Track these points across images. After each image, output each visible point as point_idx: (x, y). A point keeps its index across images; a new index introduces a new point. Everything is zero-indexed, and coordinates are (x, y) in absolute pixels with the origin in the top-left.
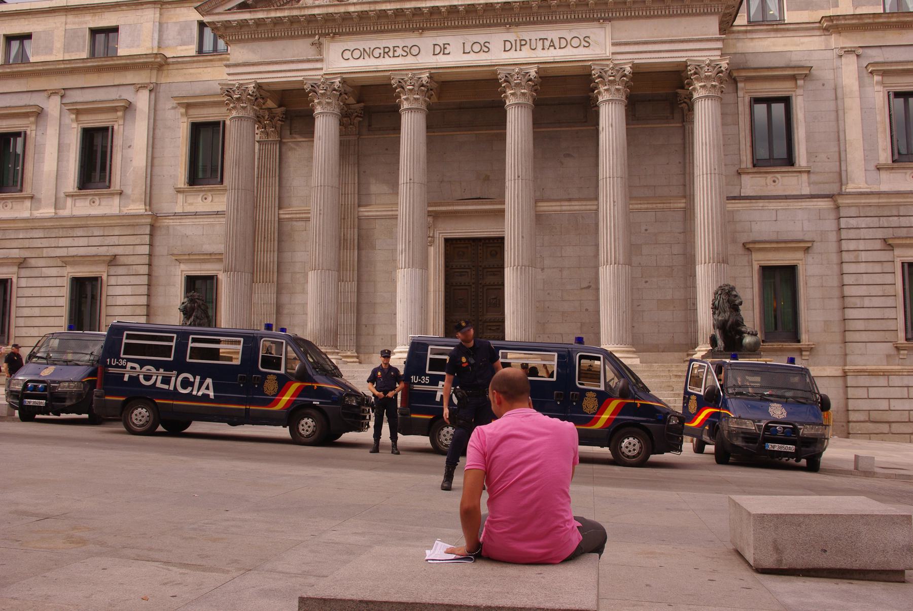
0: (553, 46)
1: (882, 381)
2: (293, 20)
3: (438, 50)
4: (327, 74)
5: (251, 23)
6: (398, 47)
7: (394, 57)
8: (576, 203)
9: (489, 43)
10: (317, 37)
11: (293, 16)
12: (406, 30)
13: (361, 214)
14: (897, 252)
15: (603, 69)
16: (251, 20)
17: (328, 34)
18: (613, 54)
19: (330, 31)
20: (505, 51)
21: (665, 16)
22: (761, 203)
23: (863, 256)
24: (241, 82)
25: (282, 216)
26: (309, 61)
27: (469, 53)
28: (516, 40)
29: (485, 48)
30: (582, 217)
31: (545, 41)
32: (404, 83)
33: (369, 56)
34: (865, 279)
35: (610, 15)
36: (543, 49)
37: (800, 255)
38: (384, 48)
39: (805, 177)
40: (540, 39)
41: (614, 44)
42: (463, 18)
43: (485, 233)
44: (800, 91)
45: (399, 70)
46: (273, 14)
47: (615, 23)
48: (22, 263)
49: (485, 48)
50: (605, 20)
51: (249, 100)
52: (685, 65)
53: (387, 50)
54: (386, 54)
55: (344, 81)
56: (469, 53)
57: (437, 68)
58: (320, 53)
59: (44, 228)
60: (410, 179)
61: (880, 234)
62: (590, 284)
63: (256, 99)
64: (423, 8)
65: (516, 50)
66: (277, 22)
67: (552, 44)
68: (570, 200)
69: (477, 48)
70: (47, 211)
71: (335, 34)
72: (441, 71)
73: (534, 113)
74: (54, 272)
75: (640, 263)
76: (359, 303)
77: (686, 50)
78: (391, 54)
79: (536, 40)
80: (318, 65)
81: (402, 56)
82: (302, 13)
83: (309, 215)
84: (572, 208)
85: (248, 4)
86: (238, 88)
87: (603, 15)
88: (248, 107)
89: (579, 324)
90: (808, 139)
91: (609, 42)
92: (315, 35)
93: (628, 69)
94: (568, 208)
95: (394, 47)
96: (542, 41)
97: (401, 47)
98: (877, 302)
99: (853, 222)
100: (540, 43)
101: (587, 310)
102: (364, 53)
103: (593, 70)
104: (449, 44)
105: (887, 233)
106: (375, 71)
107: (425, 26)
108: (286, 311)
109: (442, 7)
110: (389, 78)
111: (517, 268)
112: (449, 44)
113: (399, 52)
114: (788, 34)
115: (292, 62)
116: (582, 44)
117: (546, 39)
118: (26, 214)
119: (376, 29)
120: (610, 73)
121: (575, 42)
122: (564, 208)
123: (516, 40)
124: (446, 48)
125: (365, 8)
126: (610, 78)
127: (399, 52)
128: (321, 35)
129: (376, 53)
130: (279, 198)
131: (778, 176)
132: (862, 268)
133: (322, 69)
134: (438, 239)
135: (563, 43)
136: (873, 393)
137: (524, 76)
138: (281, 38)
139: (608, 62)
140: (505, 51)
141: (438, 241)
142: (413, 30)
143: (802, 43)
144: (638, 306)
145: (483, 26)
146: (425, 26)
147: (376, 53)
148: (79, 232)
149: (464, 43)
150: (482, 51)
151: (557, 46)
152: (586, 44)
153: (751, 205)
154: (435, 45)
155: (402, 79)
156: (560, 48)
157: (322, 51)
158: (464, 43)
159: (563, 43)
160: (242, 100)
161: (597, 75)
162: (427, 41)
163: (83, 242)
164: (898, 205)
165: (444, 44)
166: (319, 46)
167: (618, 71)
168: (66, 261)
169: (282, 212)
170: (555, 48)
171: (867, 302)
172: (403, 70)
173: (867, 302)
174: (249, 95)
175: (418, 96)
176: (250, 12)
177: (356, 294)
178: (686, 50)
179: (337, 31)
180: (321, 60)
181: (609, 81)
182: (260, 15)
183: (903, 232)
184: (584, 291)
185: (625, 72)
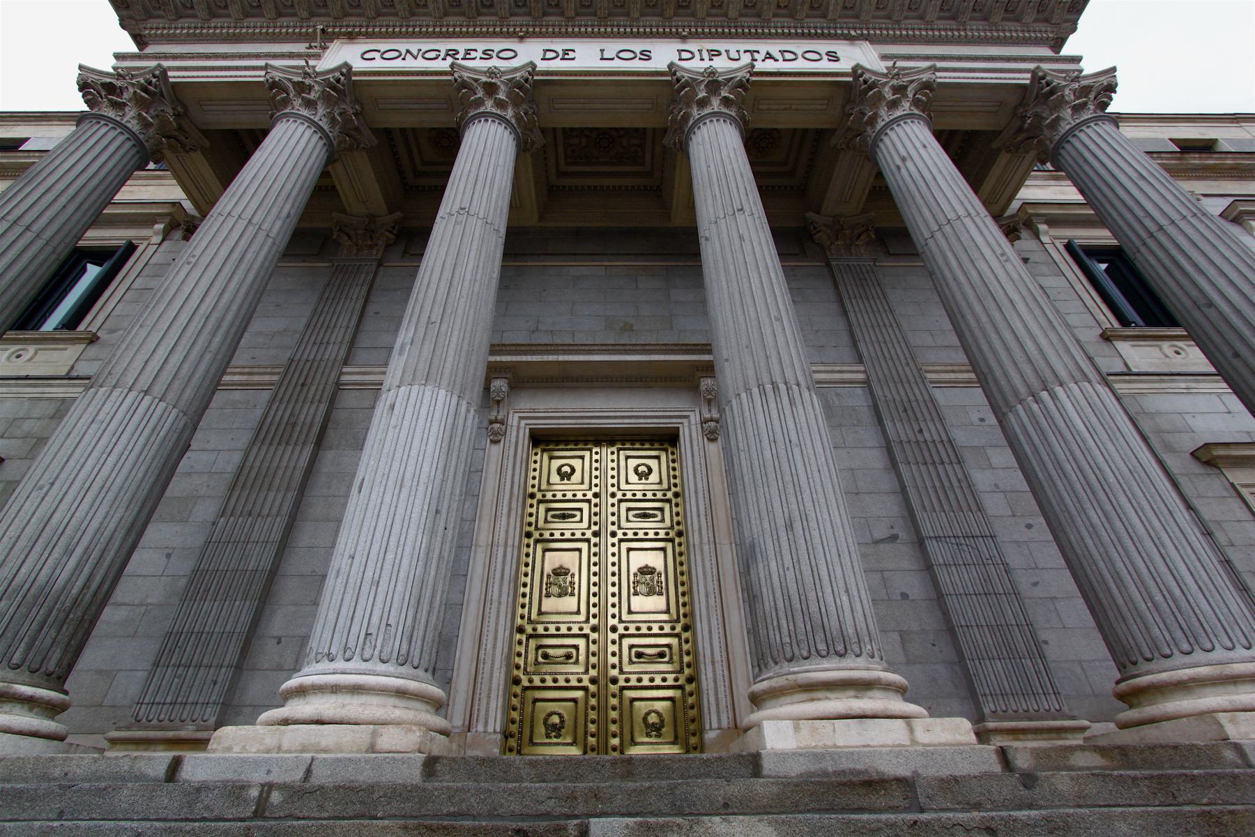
13: (345, 378)
22: (1182, 384)
27: (613, 59)
30: (837, 395)
31: (755, 54)
40: (745, 52)
56: (613, 59)
62: (895, 531)
75: (996, 486)
76: (273, 574)
89: (896, 636)
101: (905, 596)
134: (515, 429)
141: (514, 434)
144: (1036, 584)
153: (1164, 385)
177: (274, 549)
184: (881, 546)
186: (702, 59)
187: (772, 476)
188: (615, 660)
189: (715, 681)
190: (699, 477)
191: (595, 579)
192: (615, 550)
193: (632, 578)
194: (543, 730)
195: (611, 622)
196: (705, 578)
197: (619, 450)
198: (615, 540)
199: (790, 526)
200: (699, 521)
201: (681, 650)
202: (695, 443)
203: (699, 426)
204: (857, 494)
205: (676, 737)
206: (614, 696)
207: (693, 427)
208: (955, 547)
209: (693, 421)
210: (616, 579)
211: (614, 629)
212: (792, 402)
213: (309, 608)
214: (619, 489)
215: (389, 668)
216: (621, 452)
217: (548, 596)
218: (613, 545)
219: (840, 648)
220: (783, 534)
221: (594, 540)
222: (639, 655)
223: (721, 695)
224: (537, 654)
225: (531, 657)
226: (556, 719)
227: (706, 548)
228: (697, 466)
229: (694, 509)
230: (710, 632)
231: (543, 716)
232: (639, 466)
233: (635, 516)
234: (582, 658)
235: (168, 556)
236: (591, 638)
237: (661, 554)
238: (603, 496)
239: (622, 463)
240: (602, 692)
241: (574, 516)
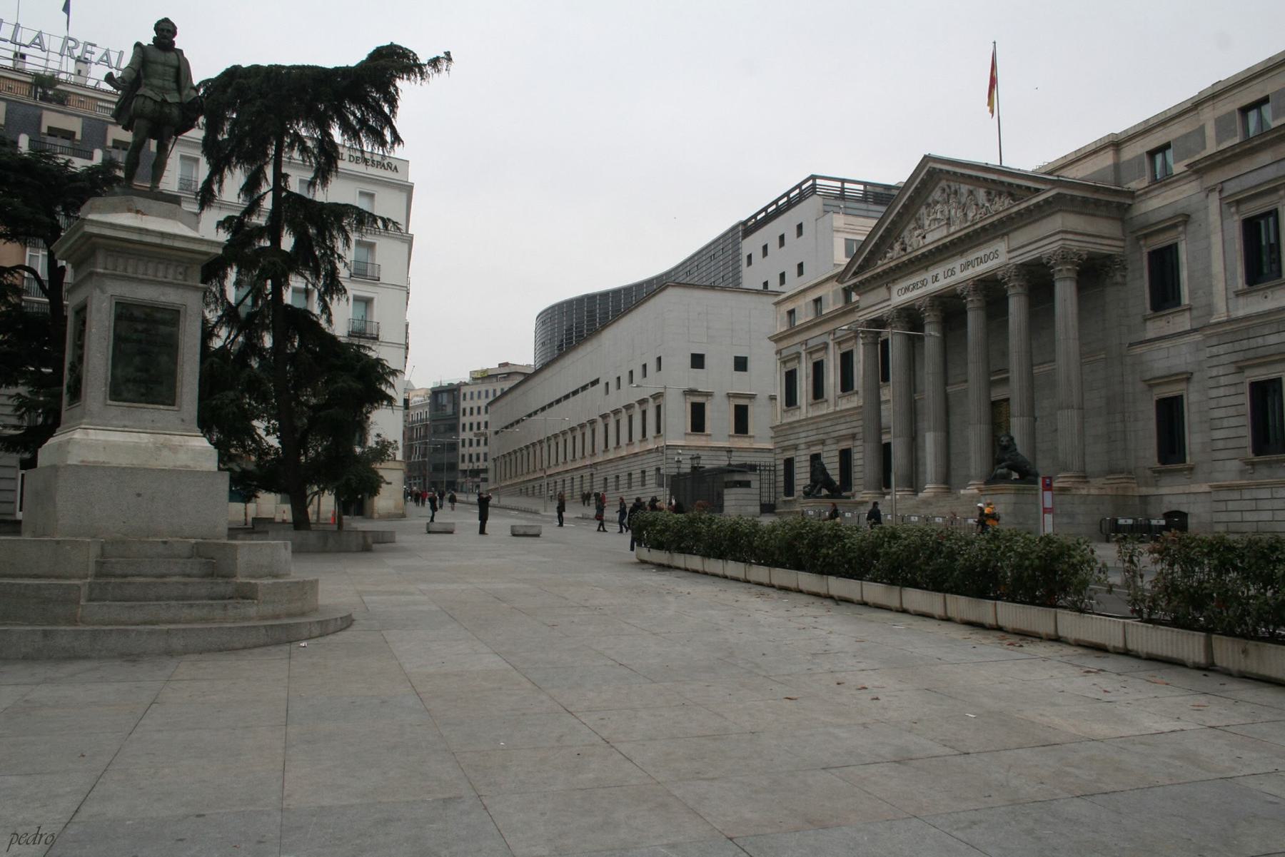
1: (1236, 495)
2: (873, 277)
14: (1248, 373)
18: (1010, 259)
22: (1158, 344)
23: (1223, 381)
26: (885, 301)
29: (953, 272)
34: (1224, 402)
37: (1183, 386)
39: (1187, 314)
44: (1183, 237)
48: (823, 442)
50: (1003, 235)
52: (1040, 258)
59: (831, 419)
61: (1234, 358)
70: (831, 409)
74: (834, 447)
90: (1190, 277)
98: (1233, 422)
99: (1215, 350)
102: (907, 289)
105: (1240, 356)
110: (914, 305)
113: (920, 285)
114: (1173, 186)
118: (825, 412)
127: (920, 285)
131: (1170, 317)
132: (1222, 392)
136: (1231, 506)
142: (922, 268)
143: (1184, 191)
148: (842, 420)
162: (928, 275)
163: (843, 426)
164: (1248, 328)
166: (889, 289)
168: (839, 439)
171: (1226, 423)
173: (1226, 423)
182: (860, 278)
183: (1251, 354)
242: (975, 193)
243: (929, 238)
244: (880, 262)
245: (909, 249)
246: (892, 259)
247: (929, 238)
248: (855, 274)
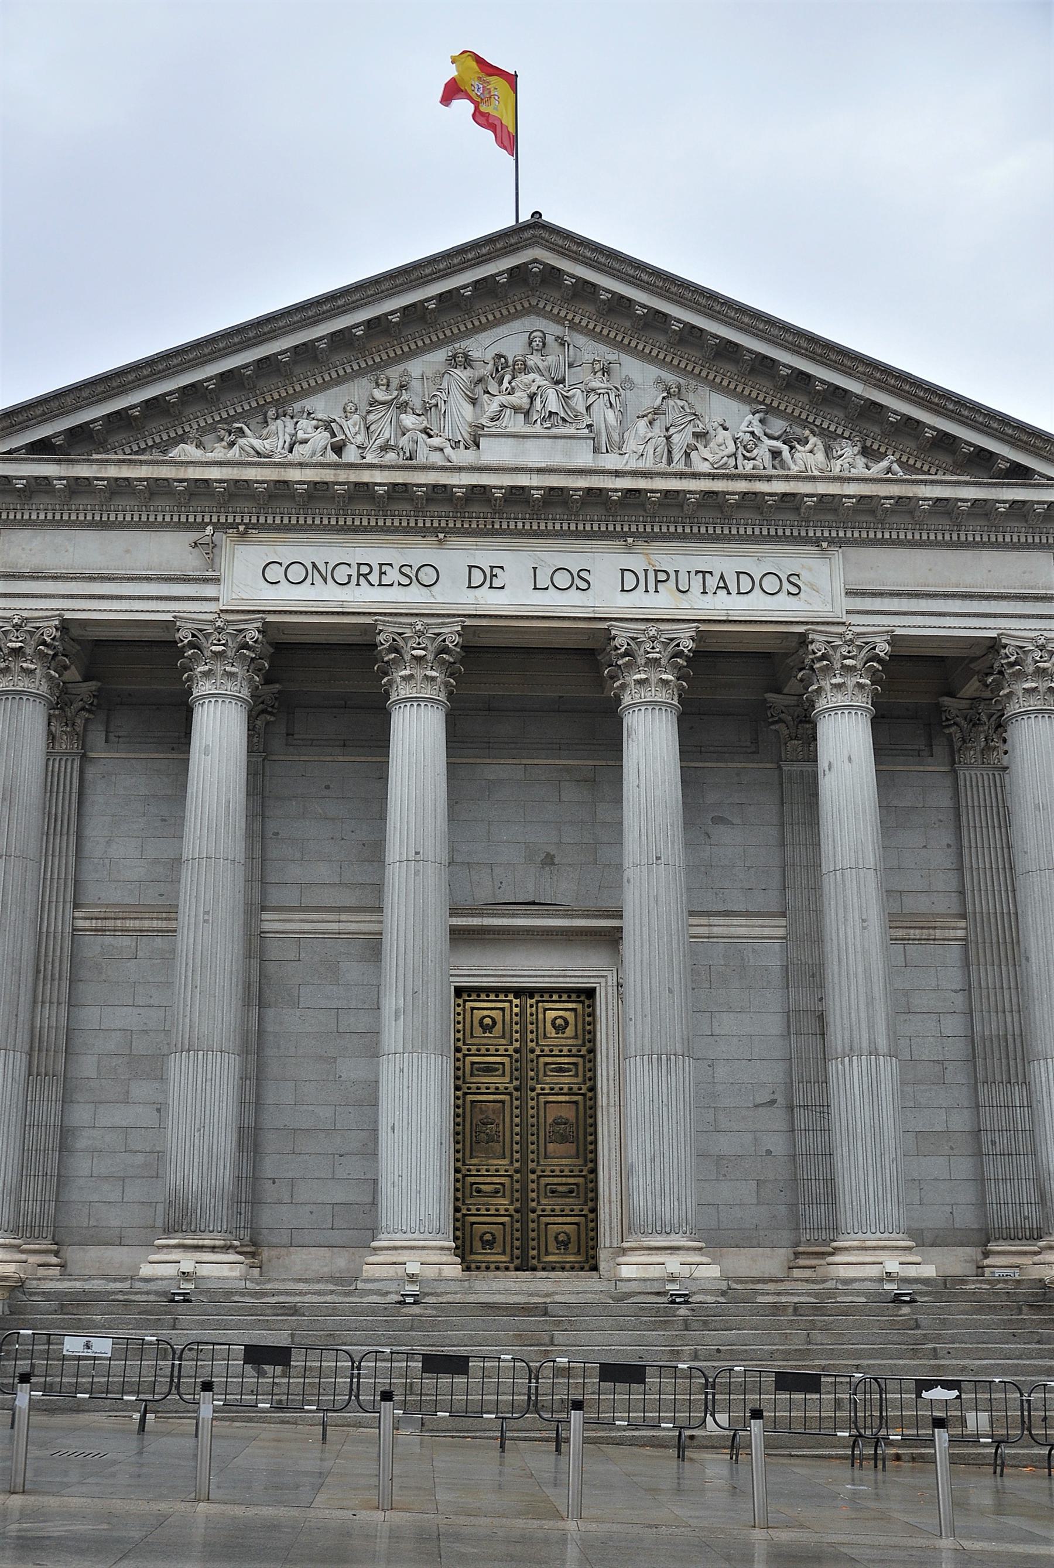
0: (726, 587)
2: (158, 488)
3: (477, 577)
4: (227, 611)
5: (59, 485)
6: (391, 565)
7: (380, 585)
8: (742, 921)
9: (589, 571)
10: (209, 530)
11: (157, 479)
12: (407, 531)
13: (267, 926)
15: (829, 643)
16: (61, 478)
17: (234, 526)
18: (848, 612)
19: (238, 520)
20: (623, 590)
21: (950, 545)
24: (26, 614)
25: (80, 924)
26: (186, 579)
27: (547, 589)
28: (646, 571)
30: (754, 951)
31: (707, 575)
32: (401, 643)
33: (325, 580)
35: (841, 534)
36: (704, 592)
38: (359, 564)
40: (697, 572)
41: (850, 593)
42: (536, 515)
43: (547, 980)
45: (391, 614)
46: (113, 472)
47: (852, 552)
49: (581, 581)
50: (832, 542)
51: (42, 655)
53: (365, 570)
54: (362, 579)
55: (266, 629)
56: (547, 589)
57: (475, 616)
58: (212, 564)
60: (417, 853)
62: (775, 1097)
63: (55, 655)
64: (455, 486)
65: (647, 591)
66: (120, 487)
67: (722, 584)
68: (727, 914)
69: (562, 580)
71: (248, 526)
72: (484, 622)
73: (683, 720)
77: (995, 616)
78: (374, 578)
79: (689, 572)
80: (209, 591)
81: (400, 584)
82: (181, 476)
83: (173, 924)
84: (733, 931)
85: (53, 445)
86: (17, 627)
87: (826, 534)
88: (38, 671)
91: (839, 588)
92: (207, 524)
93: (883, 649)
94: (724, 931)
95: (381, 565)
96: (701, 575)
97: (397, 567)
100: (697, 581)
101: (769, 1152)
103: (812, 642)
104: (502, 568)
106: (338, 613)
107: (451, 525)
108: (81, 1143)
109: (495, 487)
110: (371, 630)
111: (659, 1059)
112: (502, 568)
113: (393, 575)
115: (148, 579)
116: (784, 589)
117: (711, 573)
119: (341, 522)
120: (844, 651)
121: (771, 583)
122: (716, 930)
123: (646, 571)
124: (496, 576)
125: (327, 475)
126: (847, 662)
127: (393, 575)
128: (218, 527)
129: (341, 574)
130: (76, 882)
133: (217, 599)
135: (746, 584)
137: (666, 645)
138: (122, 526)
139: (841, 629)
140: (623, 590)
142: (424, 532)
145: (576, 535)
146: (451, 525)
147: (341, 574)
149: (535, 568)
150: (574, 587)
151: (733, 589)
152: (795, 590)
154: (470, 567)
155: (400, 634)
156: (739, 593)
157: (217, 560)
158: (535, 568)
159: (746, 584)
160: (24, 655)
161: (820, 654)
165: (492, 567)
166: (210, 549)
167: (860, 648)
169: (80, 915)
170: (729, 593)
172: (401, 614)
174: (44, 643)
175: (434, 674)
176: (59, 462)
178: (995, 616)
179: (254, 521)
180: (216, 581)
181: (844, 667)
182: (83, 471)
185: (877, 651)
186: (647, 591)
187: (648, 1125)
188: (534, 1195)
189: (610, 1215)
190: (611, 1043)
191: (517, 1129)
192: (534, 1103)
193: (548, 1127)
194: (480, 1244)
195: (531, 1165)
196: (609, 1136)
197: (538, 1002)
198: (534, 1094)
199: (653, 1160)
200: (608, 1085)
201: (586, 1188)
202: (610, 1007)
203: (615, 988)
204: (750, 1060)
205: (579, 1250)
206: (533, 1222)
207: (610, 989)
208: (818, 1114)
209: (610, 979)
210: (534, 1120)
211: (533, 1172)
212: (669, 1072)
213: (290, 1156)
214: (537, 1044)
215: (427, 1235)
216: (540, 1004)
217: (478, 1142)
218: (532, 1099)
219: (668, 1230)
220: (648, 1164)
221: (516, 1094)
222: (553, 1192)
223: (614, 1225)
224: (471, 1189)
225: (468, 1191)
226: (488, 1237)
227: (612, 1110)
228: (611, 1032)
229: (605, 1074)
230: (610, 1179)
231: (479, 1234)
232: (556, 1018)
233: (552, 1070)
234: (508, 1193)
235: (159, 1110)
236: (515, 1178)
237: (574, 1107)
238: (524, 1051)
239: (541, 1016)
240: (525, 1219)
241: (497, 1070)
242: (691, 398)
243: (494, 451)
244: (188, 451)
245: (351, 455)
246: (262, 459)
247: (494, 451)
248: (42, 448)
